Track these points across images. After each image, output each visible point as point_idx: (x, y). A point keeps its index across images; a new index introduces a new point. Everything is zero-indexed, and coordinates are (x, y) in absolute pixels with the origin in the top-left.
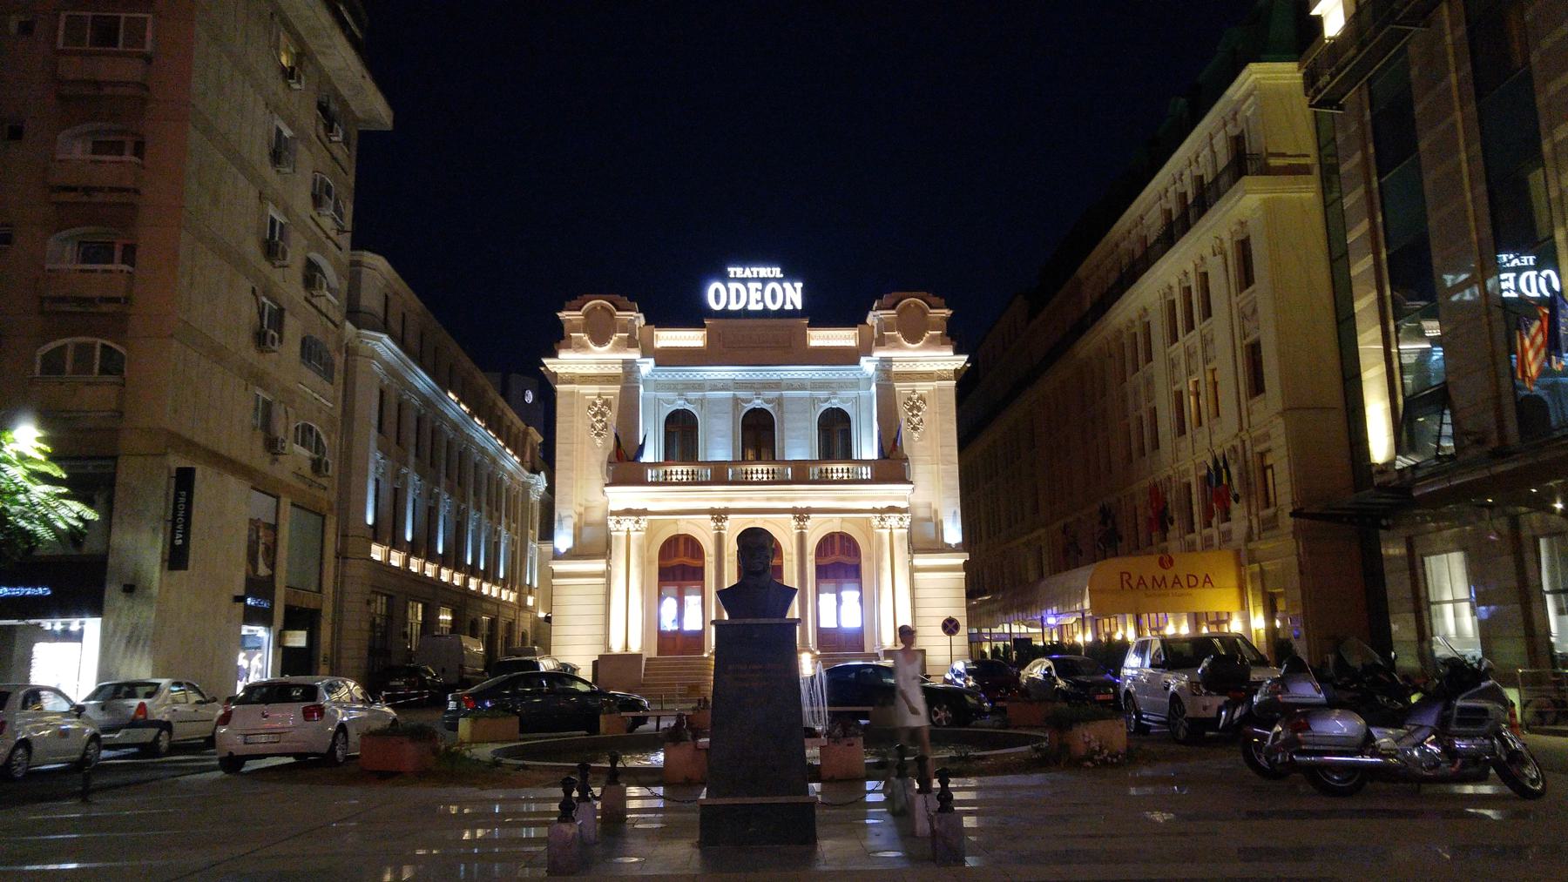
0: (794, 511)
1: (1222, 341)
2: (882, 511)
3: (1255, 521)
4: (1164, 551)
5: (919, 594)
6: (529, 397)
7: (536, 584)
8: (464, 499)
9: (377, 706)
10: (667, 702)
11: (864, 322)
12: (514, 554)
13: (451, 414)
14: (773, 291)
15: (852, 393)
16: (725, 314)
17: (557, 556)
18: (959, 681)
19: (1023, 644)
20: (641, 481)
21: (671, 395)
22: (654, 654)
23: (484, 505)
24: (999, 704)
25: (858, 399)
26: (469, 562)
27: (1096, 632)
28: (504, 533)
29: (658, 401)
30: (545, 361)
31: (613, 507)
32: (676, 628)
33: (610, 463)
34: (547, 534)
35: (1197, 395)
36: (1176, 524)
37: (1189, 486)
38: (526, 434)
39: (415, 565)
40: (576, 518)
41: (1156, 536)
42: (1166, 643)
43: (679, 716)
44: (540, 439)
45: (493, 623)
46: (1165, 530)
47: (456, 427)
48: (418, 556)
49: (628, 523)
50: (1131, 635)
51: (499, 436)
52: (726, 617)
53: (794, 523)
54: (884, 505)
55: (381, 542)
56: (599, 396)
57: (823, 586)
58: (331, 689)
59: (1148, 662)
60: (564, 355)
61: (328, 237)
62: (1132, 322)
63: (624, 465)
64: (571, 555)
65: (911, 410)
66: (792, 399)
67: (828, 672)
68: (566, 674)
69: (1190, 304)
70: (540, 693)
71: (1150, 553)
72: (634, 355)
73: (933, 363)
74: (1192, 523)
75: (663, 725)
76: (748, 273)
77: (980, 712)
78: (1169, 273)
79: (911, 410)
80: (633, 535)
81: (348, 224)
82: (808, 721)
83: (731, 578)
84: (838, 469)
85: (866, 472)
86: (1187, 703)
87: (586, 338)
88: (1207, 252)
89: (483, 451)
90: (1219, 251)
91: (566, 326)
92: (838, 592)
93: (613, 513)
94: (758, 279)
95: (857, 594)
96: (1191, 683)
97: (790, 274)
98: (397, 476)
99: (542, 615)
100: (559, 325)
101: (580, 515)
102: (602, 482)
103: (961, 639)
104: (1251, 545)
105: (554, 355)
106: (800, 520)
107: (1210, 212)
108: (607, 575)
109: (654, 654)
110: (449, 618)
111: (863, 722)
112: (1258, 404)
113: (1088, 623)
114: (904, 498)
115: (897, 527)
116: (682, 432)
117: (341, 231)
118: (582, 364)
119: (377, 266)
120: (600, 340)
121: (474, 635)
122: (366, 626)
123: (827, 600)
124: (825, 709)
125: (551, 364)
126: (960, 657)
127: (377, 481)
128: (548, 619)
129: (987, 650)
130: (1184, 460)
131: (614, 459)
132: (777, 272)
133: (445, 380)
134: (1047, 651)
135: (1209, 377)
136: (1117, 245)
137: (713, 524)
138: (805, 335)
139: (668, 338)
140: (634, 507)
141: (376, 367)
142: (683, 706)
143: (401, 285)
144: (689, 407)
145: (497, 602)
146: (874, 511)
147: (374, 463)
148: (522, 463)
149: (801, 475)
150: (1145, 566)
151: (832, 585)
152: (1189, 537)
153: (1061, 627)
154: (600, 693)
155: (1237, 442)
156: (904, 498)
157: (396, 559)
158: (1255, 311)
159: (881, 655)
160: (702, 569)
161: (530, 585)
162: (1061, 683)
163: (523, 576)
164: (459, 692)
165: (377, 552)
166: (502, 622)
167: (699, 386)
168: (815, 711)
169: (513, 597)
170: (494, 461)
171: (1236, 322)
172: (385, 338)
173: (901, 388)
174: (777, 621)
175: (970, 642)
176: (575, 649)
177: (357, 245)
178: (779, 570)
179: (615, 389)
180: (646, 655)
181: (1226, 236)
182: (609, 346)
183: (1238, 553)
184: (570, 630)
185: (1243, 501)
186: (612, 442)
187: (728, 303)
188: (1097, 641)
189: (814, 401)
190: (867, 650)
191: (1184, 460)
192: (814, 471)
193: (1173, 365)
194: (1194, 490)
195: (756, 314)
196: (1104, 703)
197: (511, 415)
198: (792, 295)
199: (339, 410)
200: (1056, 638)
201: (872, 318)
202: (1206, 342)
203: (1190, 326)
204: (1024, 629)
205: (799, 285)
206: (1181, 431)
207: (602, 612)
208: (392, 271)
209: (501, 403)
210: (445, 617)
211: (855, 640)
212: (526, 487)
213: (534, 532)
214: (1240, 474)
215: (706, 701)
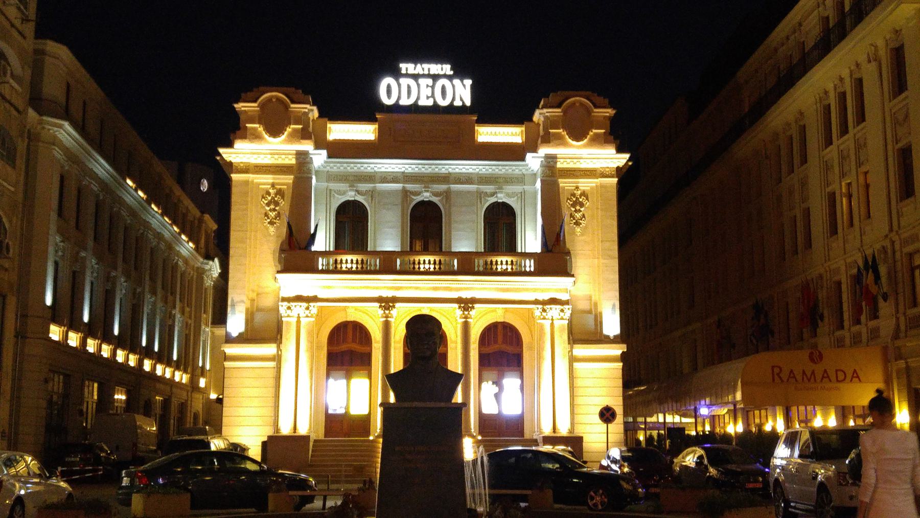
0: (459, 301)
1: (875, 144)
2: (544, 303)
3: (902, 319)
4: (815, 346)
5: (578, 383)
6: (205, 186)
7: (208, 367)
8: (140, 282)
9: (54, 481)
10: (333, 482)
11: (531, 120)
12: (187, 337)
13: (128, 199)
14: (443, 88)
15: (518, 188)
16: (396, 108)
17: (229, 340)
18: (614, 467)
19: (676, 433)
20: (313, 270)
21: (343, 186)
22: (321, 436)
23: (159, 290)
24: (653, 490)
25: (522, 196)
26: (144, 343)
27: (747, 423)
28: (178, 316)
29: (330, 192)
30: (221, 150)
31: (285, 294)
32: (342, 411)
33: (282, 250)
34: (220, 318)
35: (850, 197)
36: (826, 320)
37: (839, 284)
38: (201, 221)
39: (91, 346)
40: (248, 304)
41: (806, 333)
42: (816, 435)
43: (346, 496)
44: (215, 227)
45: (166, 403)
46: (815, 326)
47: (133, 213)
48: (94, 337)
49: (299, 308)
50: (780, 427)
51: (175, 222)
52: (392, 399)
53: (459, 312)
54: (546, 297)
55: (59, 323)
56: (273, 185)
57: (486, 374)
58: (9, 463)
59: (797, 453)
60: (239, 145)
61: (13, 26)
62: (788, 124)
63: (296, 254)
64: (242, 339)
65: (574, 205)
66: (459, 193)
67: (490, 456)
68: (236, 453)
69: (845, 109)
70: (211, 471)
71: (801, 348)
72: (307, 146)
73: (595, 161)
74: (842, 321)
75: (330, 503)
76: (420, 69)
77: (634, 497)
78: (825, 77)
79: (574, 205)
80: (304, 321)
81: (32, 12)
82: (470, 504)
83: (397, 364)
84: (503, 261)
85: (529, 265)
86: (834, 493)
87: (261, 129)
88: (862, 58)
89: (159, 236)
90: (874, 58)
91: (242, 117)
92: (498, 383)
93: (284, 300)
94: (429, 76)
95: (519, 381)
96: (838, 473)
97: (459, 72)
98: (76, 259)
99: (213, 396)
100: (236, 115)
101: (253, 300)
102: (274, 269)
103: (617, 427)
104: (898, 343)
105: (230, 145)
106: (466, 309)
107: (867, 19)
108: (277, 359)
109: (321, 436)
110: (123, 397)
111: (523, 505)
112: (908, 207)
113: (739, 415)
114: (566, 291)
115: (559, 318)
116: (352, 223)
117: (25, 20)
118: (256, 155)
119: (60, 55)
120: (275, 131)
121: (147, 413)
122: (43, 404)
123: (489, 388)
124: (484, 491)
125: (226, 154)
126: (617, 444)
127: (56, 264)
128: (220, 401)
129: (641, 437)
130: (835, 259)
131: (286, 247)
132: (447, 69)
133: (123, 168)
134: (699, 440)
135: (861, 179)
136: (776, 50)
137: (381, 312)
138: (472, 133)
139: (339, 131)
140: (305, 294)
141: (57, 153)
142: (349, 486)
143: (82, 73)
144: (360, 198)
145: (171, 382)
146: (536, 302)
147: (54, 245)
148: (197, 249)
149: (467, 266)
150: (794, 360)
151: (493, 374)
152: (838, 333)
153: (713, 419)
154: (270, 473)
155: (887, 243)
156: (566, 291)
157: (74, 340)
158: (907, 116)
159: (540, 441)
160: (369, 356)
161: (203, 367)
162: (712, 471)
163: (195, 359)
164: (132, 469)
165: (55, 333)
166: (175, 402)
167: (370, 178)
168: (478, 494)
169: (185, 378)
170: (170, 247)
171: (888, 124)
172: (67, 125)
173: (565, 184)
174: (443, 405)
175: (626, 430)
176: (246, 428)
177: (41, 33)
178: (444, 356)
179: (289, 179)
180: (313, 437)
181: (880, 43)
182: (283, 137)
183: (885, 349)
184: (242, 411)
185: (891, 300)
186: (284, 230)
187: (399, 98)
188: (747, 432)
189: (480, 195)
190: (527, 435)
191: (835, 259)
192: (479, 263)
193: (827, 168)
194: (844, 287)
195: (425, 109)
196: (753, 490)
197: (187, 203)
198: (461, 92)
199: (20, 197)
200: (708, 428)
201: (538, 116)
202: (860, 146)
203: (844, 131)
204: (677, 419)
205: (468, 82)
206: (834, 231)
207: (274, 393)
208: (71, 55)
209: (178, 191)
210: (120, 397)
211: (515, 427)
212: (201, 273)
213: (208, 316)
214: (889, 273)
215: (371, 482)
